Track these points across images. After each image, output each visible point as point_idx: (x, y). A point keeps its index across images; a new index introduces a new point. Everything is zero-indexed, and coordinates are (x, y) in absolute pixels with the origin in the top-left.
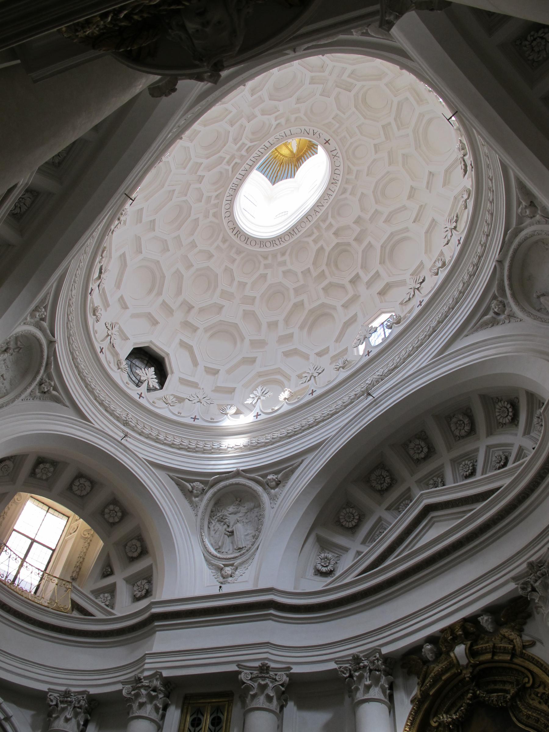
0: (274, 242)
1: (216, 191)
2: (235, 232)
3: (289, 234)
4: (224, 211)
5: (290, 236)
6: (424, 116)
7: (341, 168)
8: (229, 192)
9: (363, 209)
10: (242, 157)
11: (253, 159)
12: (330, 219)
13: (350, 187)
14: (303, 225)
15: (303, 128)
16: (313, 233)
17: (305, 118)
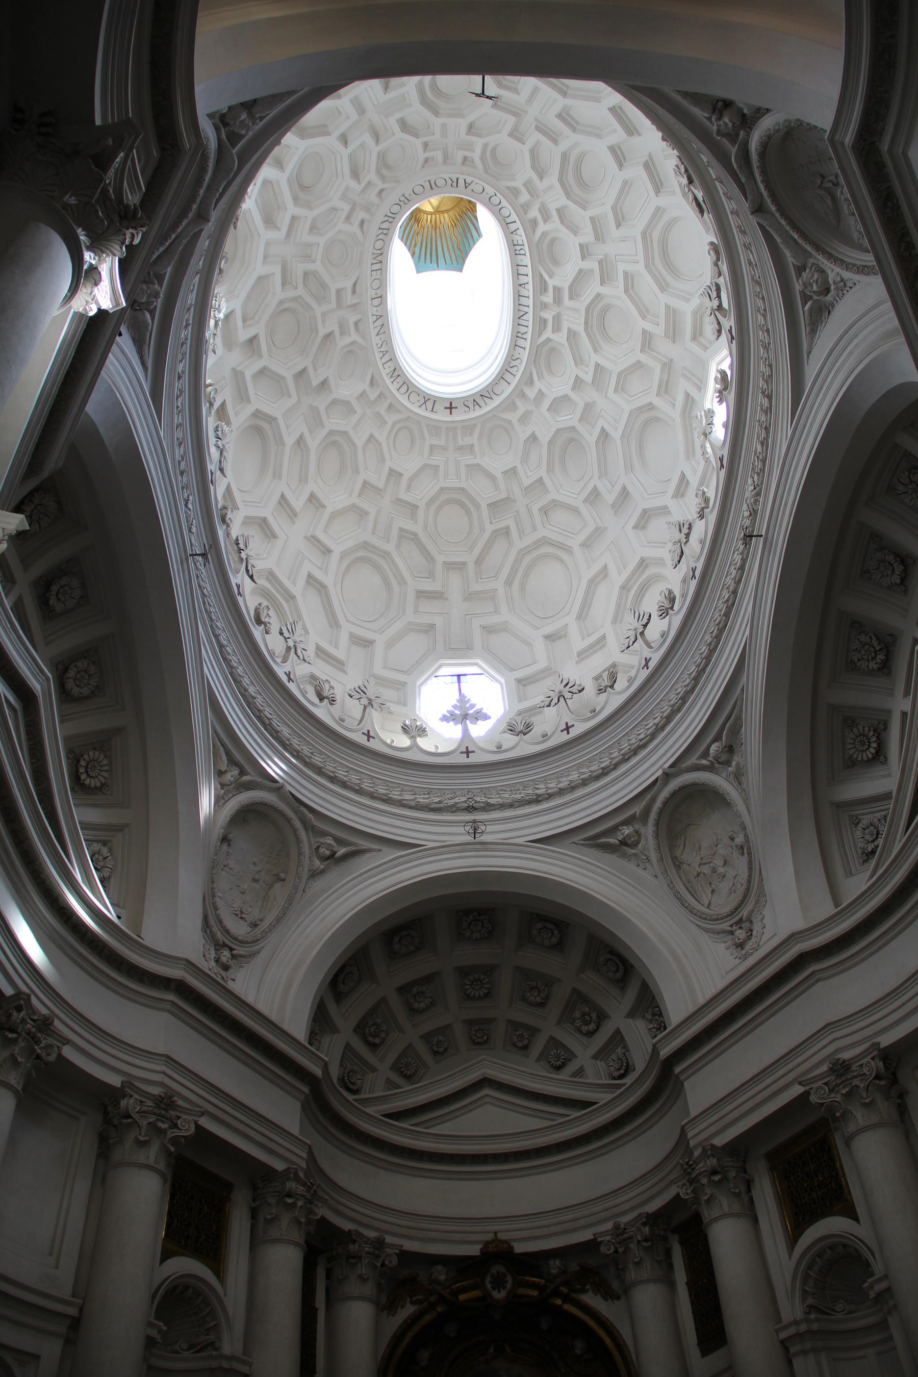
0: (391, 220)
1: (543, 233)
2: (461, 182)
3: (380, 252)
4: (504, 203)
5: (378, 252)
6: (399, 584)
7: (403, 400)
8: (521, 237)
9: (334, 402)
10: (544, 306)
11: (526, 309)
12: (354, 336)
13: (373, 395)
14: (376, 284)
15: (497, 401)
16: (354, 292)
17: (507, 416)
